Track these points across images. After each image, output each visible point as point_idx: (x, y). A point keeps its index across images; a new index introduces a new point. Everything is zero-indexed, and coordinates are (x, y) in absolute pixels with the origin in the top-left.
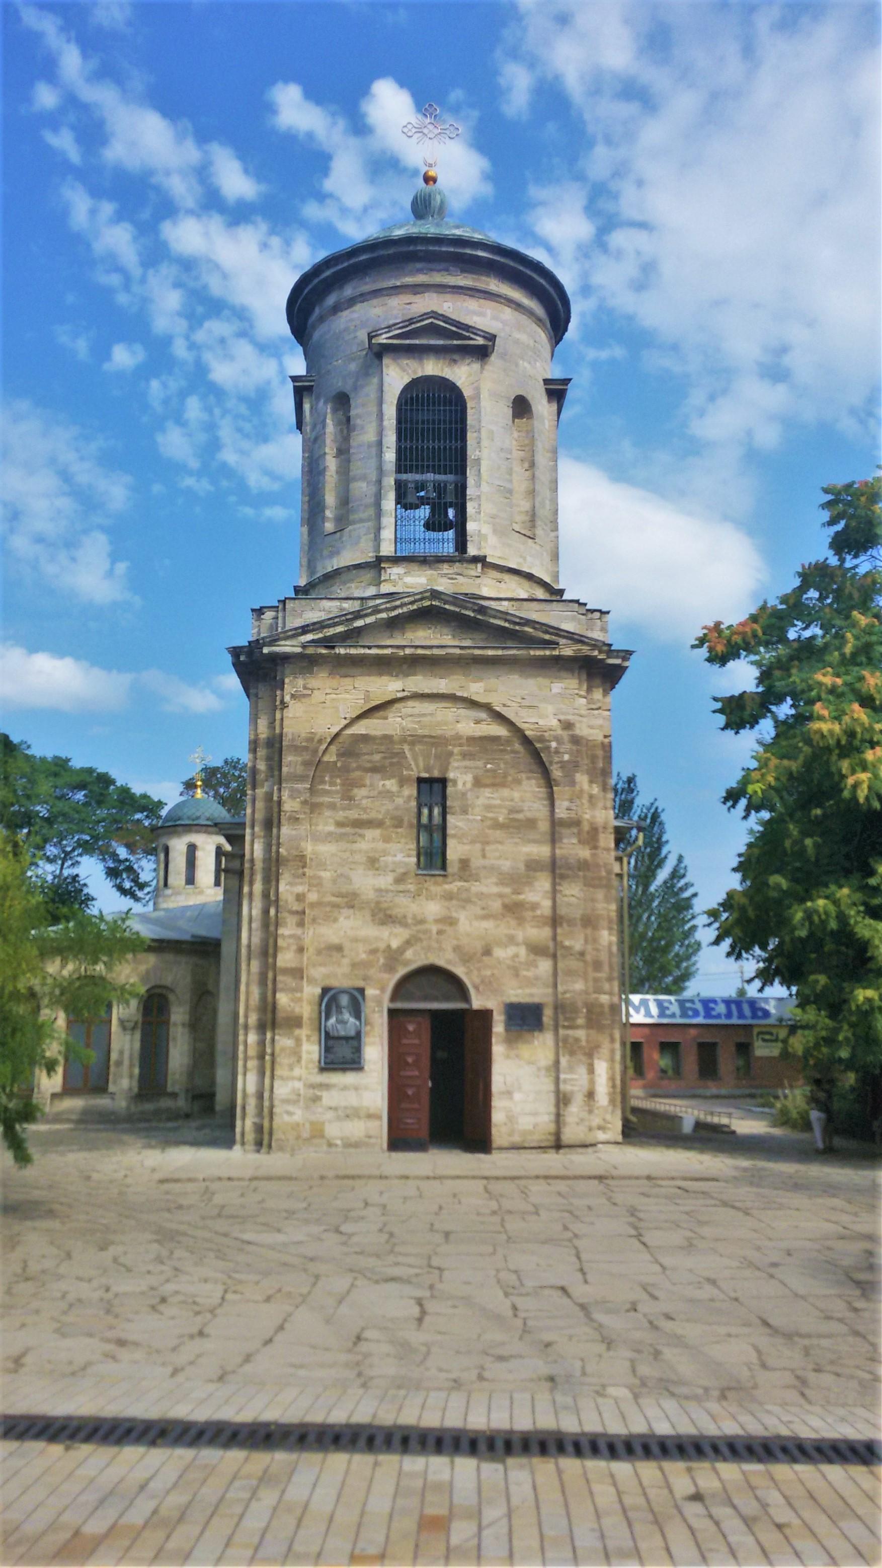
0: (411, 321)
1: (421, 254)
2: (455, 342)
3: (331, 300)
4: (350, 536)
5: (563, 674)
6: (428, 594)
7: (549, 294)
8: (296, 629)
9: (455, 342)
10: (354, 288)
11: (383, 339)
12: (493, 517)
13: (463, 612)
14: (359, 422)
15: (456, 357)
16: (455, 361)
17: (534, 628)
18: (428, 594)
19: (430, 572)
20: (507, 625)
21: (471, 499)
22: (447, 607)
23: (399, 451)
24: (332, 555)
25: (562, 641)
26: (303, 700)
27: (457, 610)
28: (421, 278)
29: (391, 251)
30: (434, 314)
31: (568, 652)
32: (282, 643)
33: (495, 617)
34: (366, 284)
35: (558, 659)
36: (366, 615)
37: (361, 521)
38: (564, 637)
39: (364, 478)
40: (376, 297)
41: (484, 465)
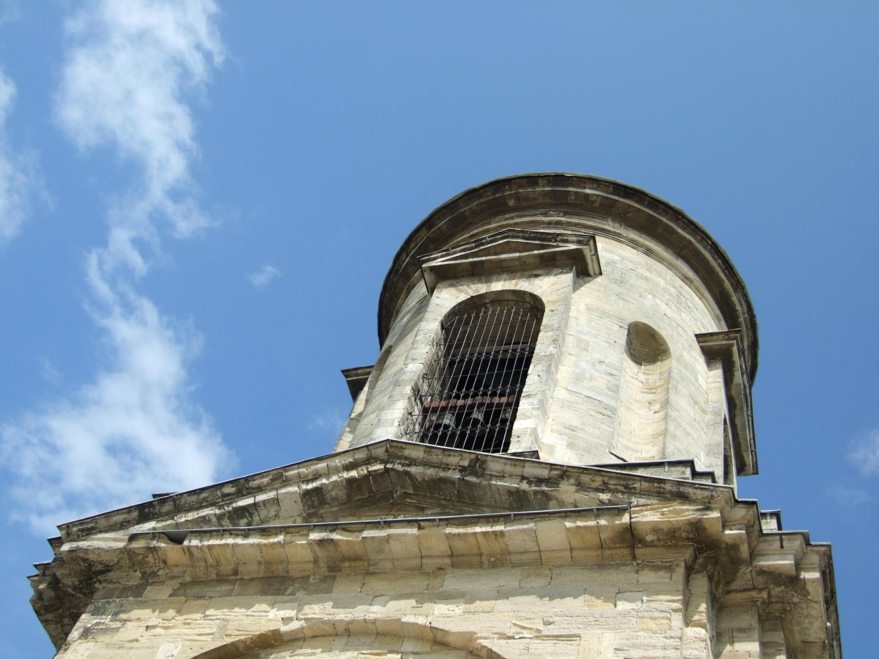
1: (511, 203)
2: (536, 252)
5: (648, 576)
6: (380, 452)
7: (704, 259)
8: (129, 510)
9: (536, 252)
12: (573, 429)
16: (536, 276)
17: (581, 486)
18: (380, 452)
20: (524, 486)
21: (529, 396)
22: (413, 470)
25: (634, 501)
26: (101, 638)
27: (430, 472)
31: (649, 515)
32: (100, 536)
33: (502, 477)
35: (630, 537)
36: (260, 489)
38: (642, 493)
41: (564, 373)
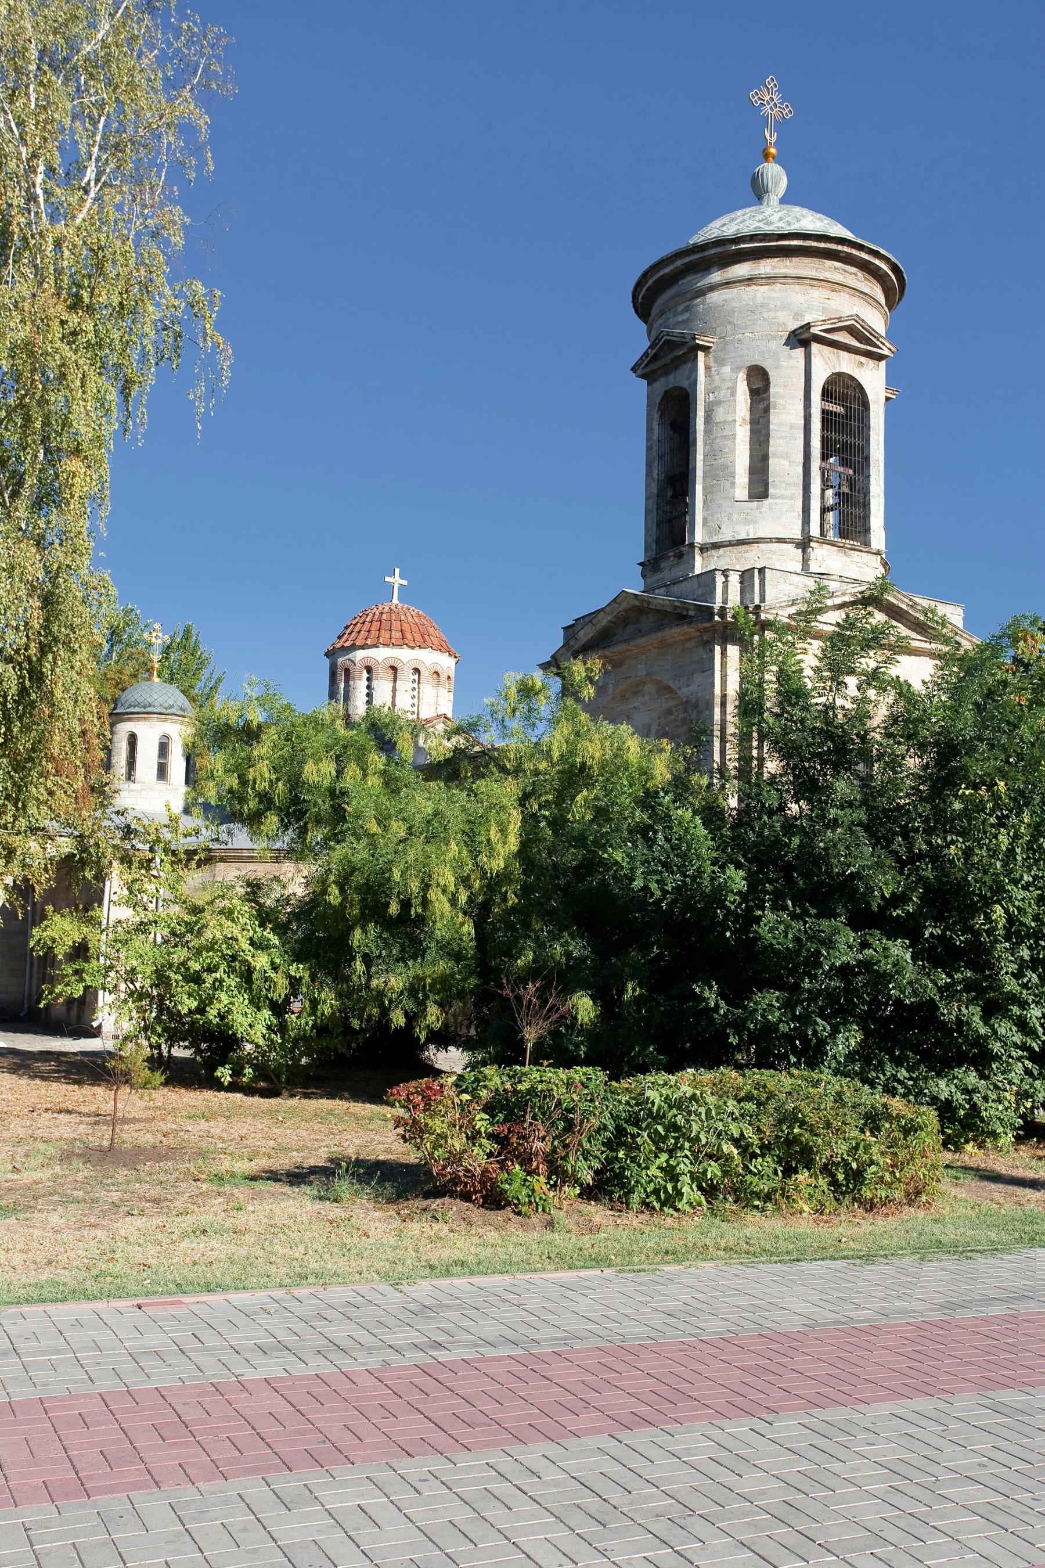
0: (840, 320)
3: (742, 270)
4: (771, 509)
10: (774, 267)
11: (815, 330)
13: (900, 605)
14: (781, 401)
15: (863, 359)
19: (845, 558)
23: (824, 440)
24: (746, 522)
28: (838, 277)
29: (822, 245)
30: (857, 318)
34: (786, 267)
37: (783, 497)
39: (786, 456)
40: (798, 284)
